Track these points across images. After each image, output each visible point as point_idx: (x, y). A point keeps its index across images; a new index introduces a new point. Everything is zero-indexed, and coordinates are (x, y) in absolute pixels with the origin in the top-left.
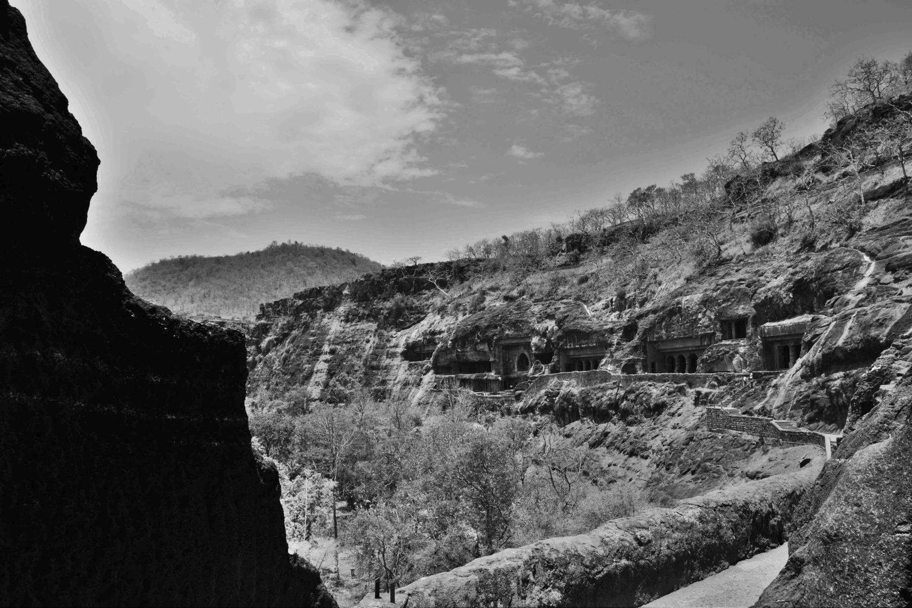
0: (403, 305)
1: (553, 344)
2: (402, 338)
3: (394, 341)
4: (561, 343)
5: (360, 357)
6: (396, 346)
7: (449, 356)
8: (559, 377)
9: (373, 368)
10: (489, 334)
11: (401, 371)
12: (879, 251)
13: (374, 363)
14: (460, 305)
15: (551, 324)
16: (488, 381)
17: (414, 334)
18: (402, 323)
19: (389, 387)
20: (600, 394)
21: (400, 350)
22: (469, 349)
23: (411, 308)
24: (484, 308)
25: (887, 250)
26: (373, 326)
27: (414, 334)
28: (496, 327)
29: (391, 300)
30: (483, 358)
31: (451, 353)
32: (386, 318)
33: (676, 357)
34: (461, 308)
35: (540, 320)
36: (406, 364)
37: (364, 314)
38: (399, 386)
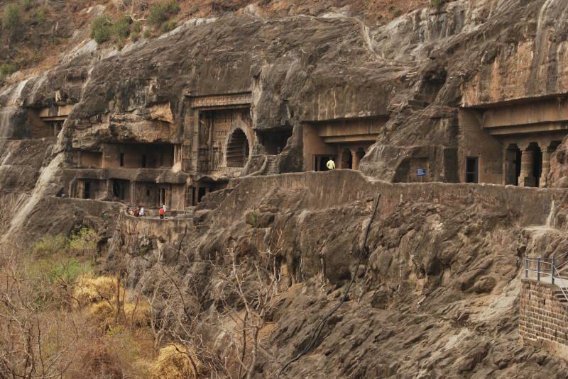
7: (96, 129)
22: (134, 115)
31: (100, 121)
33: (523, 147)
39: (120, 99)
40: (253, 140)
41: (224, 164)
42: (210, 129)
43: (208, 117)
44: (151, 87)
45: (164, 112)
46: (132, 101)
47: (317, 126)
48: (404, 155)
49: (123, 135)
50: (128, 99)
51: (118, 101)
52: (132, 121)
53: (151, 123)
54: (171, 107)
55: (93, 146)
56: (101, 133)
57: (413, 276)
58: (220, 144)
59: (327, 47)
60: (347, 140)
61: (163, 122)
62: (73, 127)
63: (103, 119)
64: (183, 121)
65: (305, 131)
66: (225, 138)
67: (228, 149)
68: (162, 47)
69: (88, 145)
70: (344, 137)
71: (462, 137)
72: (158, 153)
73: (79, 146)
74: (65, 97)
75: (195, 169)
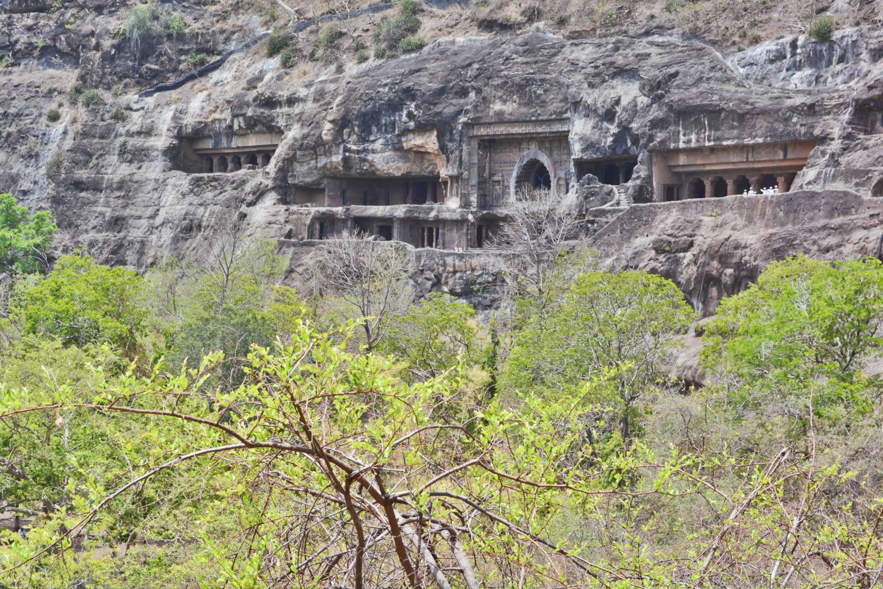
0: (157, 27)
1: (636, 141)
2: (161, 116)
3: (136, 121)
4: (660, 136)
5: (32, 156)
6: (148, 132)
7: (323, 161)
8: (683, 209)
9: (79, 185)
10: (447, 107)
11: (169, 197)
13: (82, 174)
14: (341, 35)
15: (628, 92)
16: (440, 222)
17: (197, 103)
18: (155, 74)
19: (136, 233)
20: (832, 240)
21: (161, 141)
22: (378, 145)
23: (181, 37)
24: (420, 46)
26: (67, 77)
27: (197, 103)
28: (463, 93)
29: (122, 12)
30: (416, 169)
31: (328, 153)
32: (107, 58)
34: (346, 43)
35: (596, 79)
36: (182, 180)
37: (31, 46)
38: (167, 235)
39: (359, 126)
41: (512, 198)
42: (488, 159)
43: (485, 148)
44: (405, 112)
45: (430, 142)
46: (374, 129)
47: (665, 153)
50: (370, 127)
51: (356, 129)
53: (399, 153)
54: (438, 136)
55: (314, 181)
56: (329, 166)
58: (502, 176)
59: (676, 74)
60: (708, 168)
61: (417, 152)
64: (461, 151)
65: (655, 160)
66: (512, 170)
67: (517, 182)
68: (414, 67)
69: (308, 180)
70: (704, 165)
73: (296, 181)
75: (475, 204)
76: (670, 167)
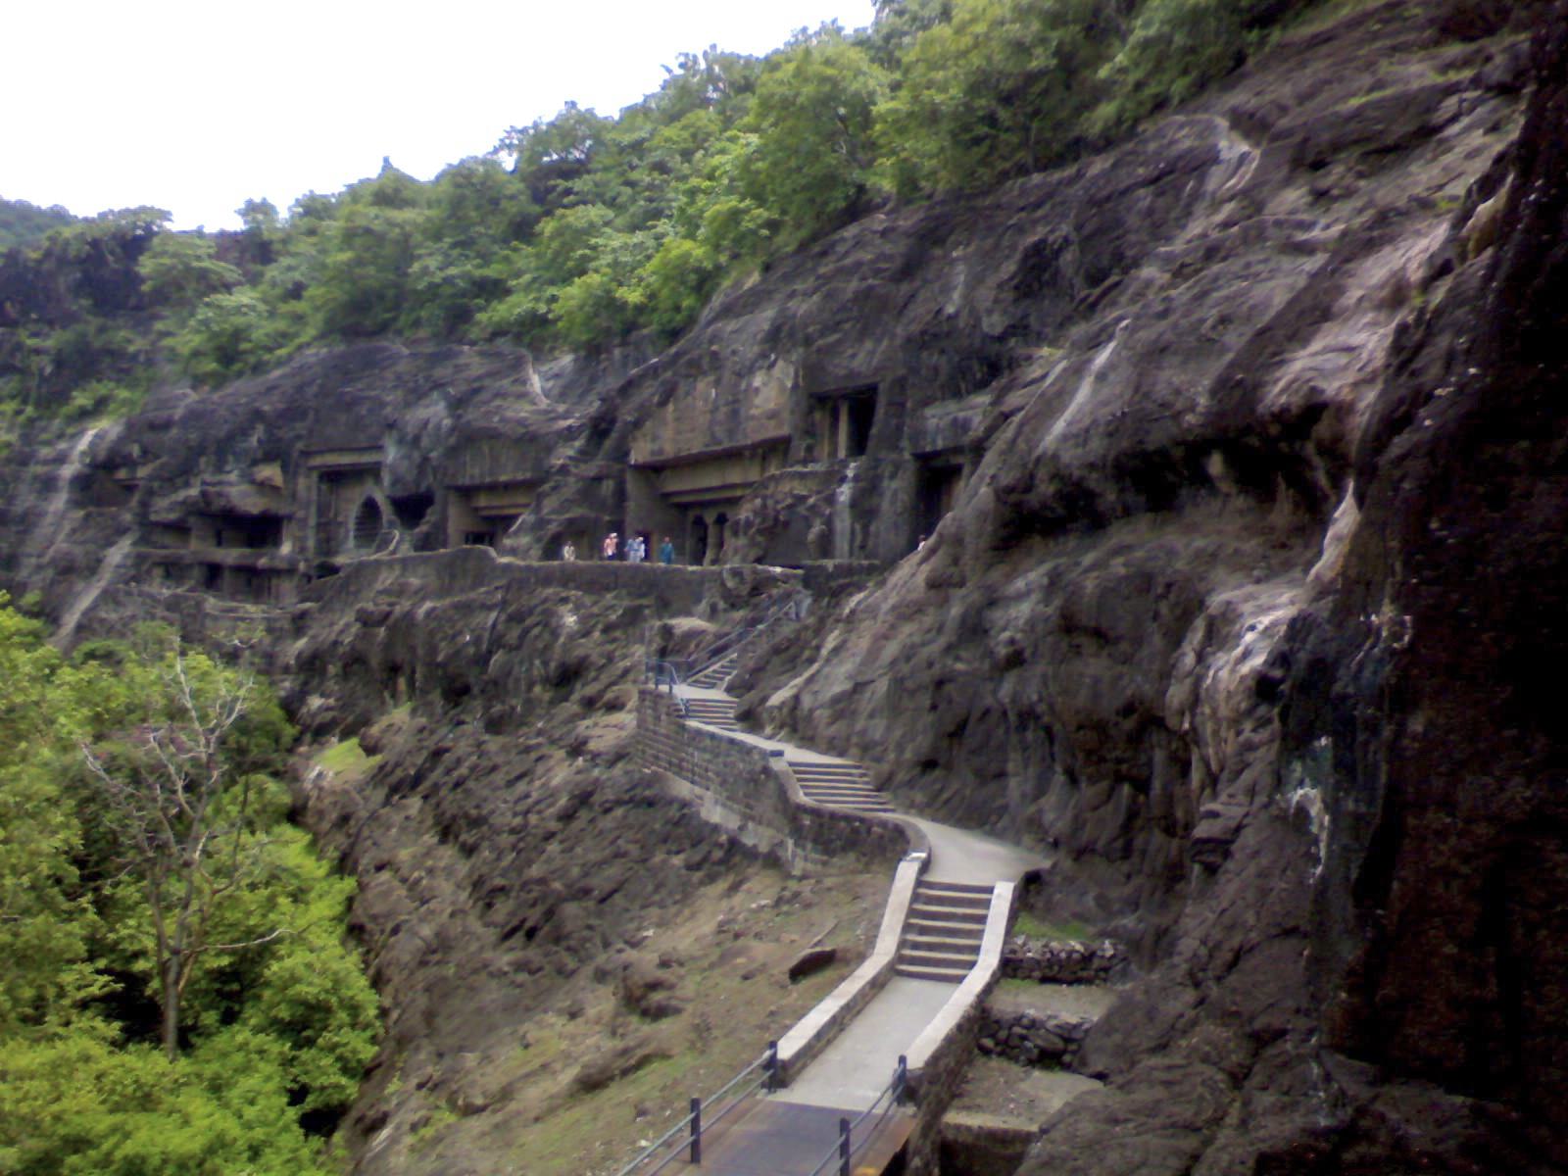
7: (181, 495)
12: (1283, 110)
22: (233, 477)
25: (1310, 105)
31: (187, 485)
40: (387, 511)
41: (351, 543)
45: (271, 472)
46: (231, 458)
47: (467, 493)
48: (553, 528)
49: (218, 504)
52: (230, 484)
57: (537, 689)
62: (151, 493)
63: (192, 480)
69: (173, 516)
71: (631, 505)
72: (262, 529)
74: (145, 452)
76: (477, 509)
